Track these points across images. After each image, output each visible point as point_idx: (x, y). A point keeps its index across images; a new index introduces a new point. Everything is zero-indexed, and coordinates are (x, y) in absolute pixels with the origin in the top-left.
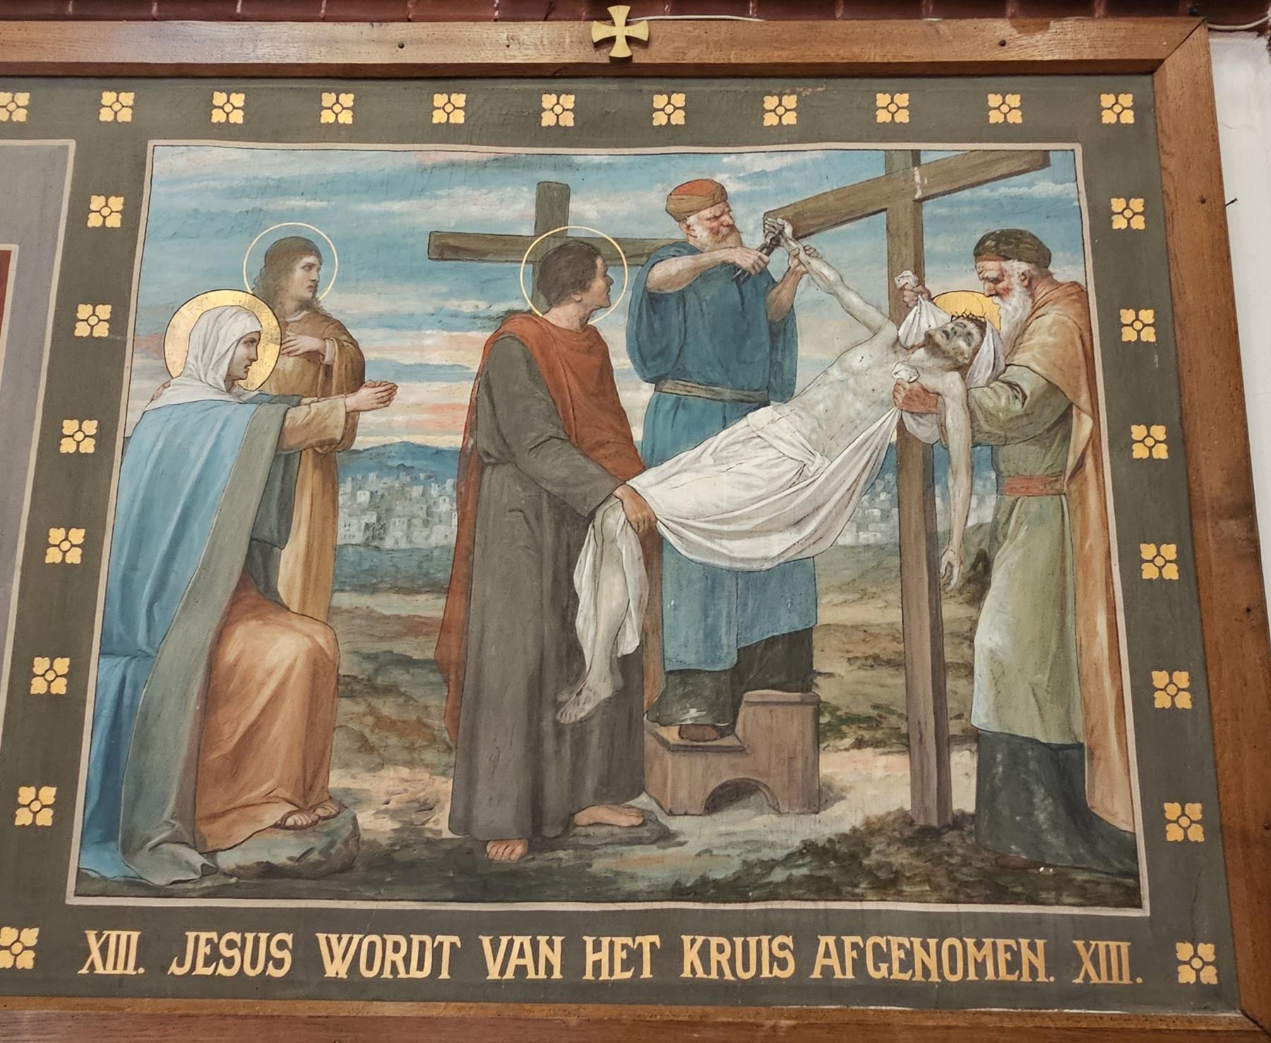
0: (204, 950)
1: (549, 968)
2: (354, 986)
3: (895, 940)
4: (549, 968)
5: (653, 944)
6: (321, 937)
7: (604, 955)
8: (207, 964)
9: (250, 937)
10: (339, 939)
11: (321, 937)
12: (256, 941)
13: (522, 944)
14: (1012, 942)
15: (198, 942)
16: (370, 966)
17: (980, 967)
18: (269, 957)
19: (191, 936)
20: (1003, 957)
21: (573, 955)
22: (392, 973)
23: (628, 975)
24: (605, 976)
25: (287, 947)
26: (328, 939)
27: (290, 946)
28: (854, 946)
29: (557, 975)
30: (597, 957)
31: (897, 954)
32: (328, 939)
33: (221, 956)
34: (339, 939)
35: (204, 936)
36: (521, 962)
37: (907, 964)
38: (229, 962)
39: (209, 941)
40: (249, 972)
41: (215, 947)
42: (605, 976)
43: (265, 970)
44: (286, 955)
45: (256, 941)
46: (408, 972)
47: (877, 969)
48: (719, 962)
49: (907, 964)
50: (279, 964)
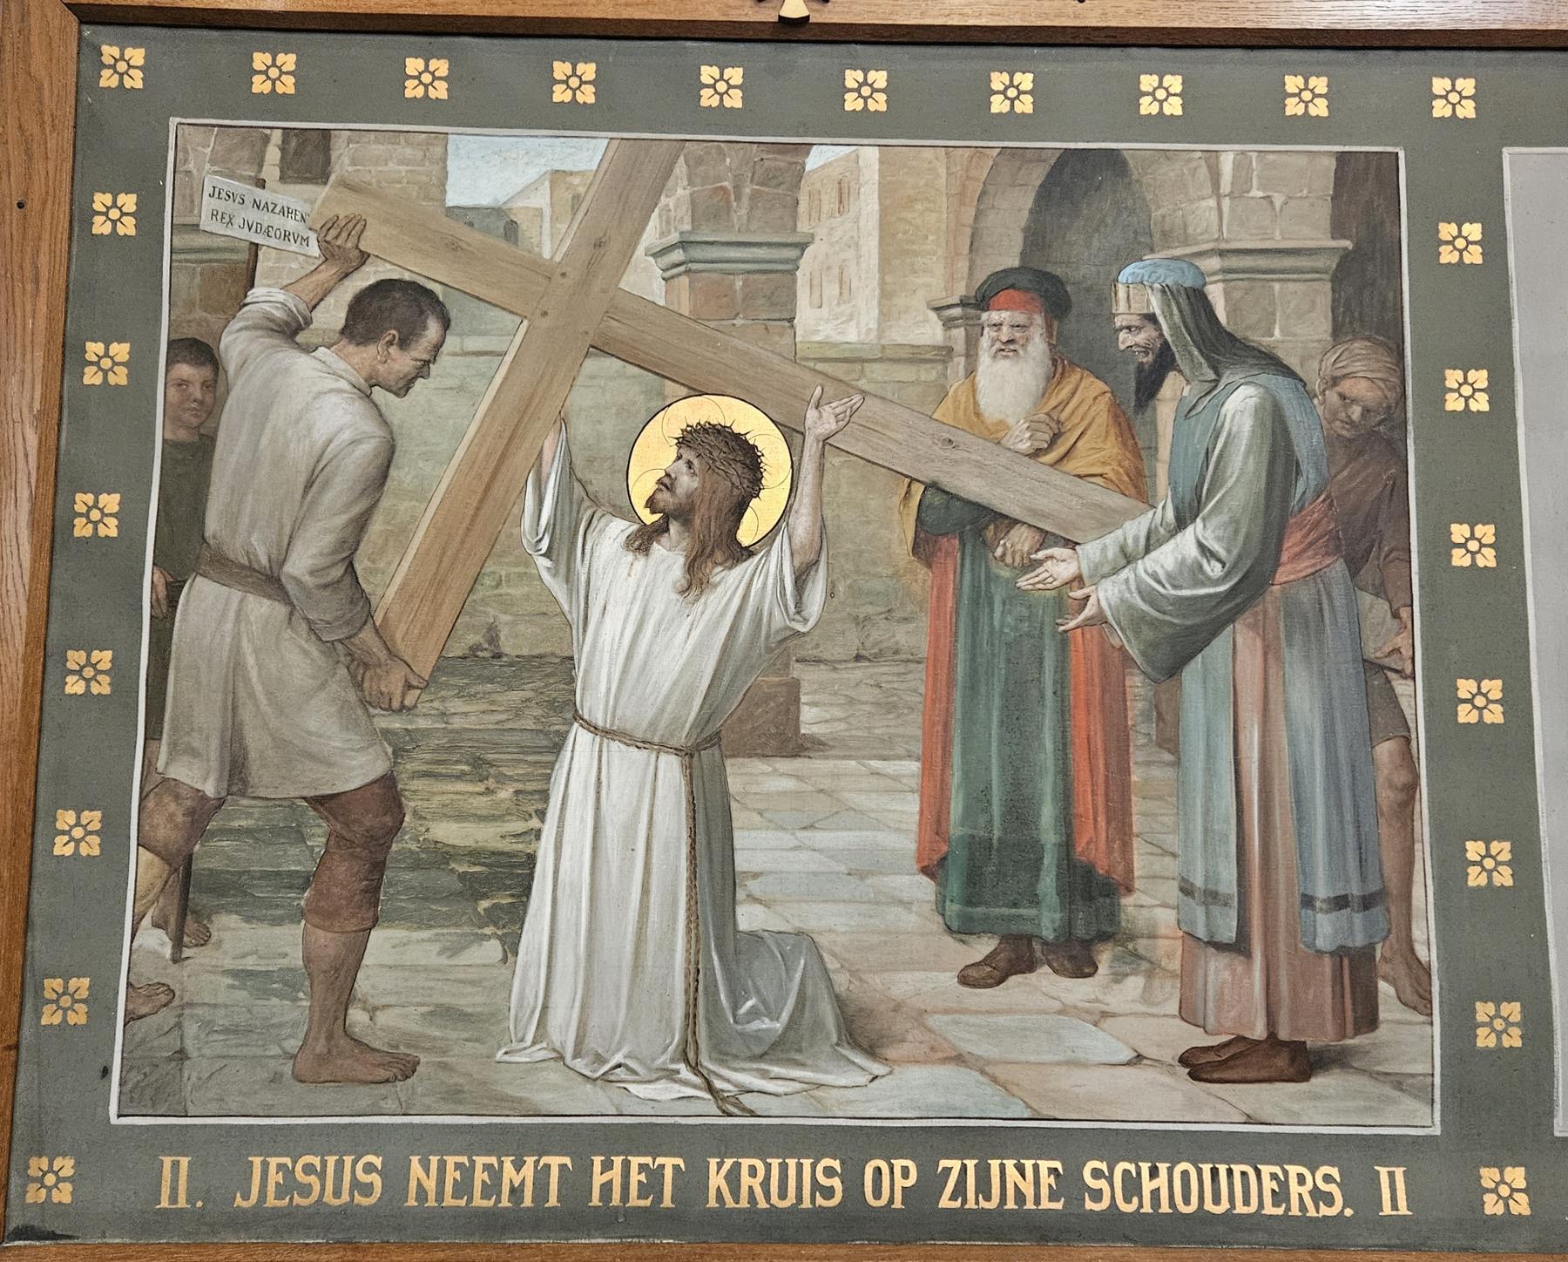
0: (275, 1177)
39: (280, 1167)
41: (288, 1173)
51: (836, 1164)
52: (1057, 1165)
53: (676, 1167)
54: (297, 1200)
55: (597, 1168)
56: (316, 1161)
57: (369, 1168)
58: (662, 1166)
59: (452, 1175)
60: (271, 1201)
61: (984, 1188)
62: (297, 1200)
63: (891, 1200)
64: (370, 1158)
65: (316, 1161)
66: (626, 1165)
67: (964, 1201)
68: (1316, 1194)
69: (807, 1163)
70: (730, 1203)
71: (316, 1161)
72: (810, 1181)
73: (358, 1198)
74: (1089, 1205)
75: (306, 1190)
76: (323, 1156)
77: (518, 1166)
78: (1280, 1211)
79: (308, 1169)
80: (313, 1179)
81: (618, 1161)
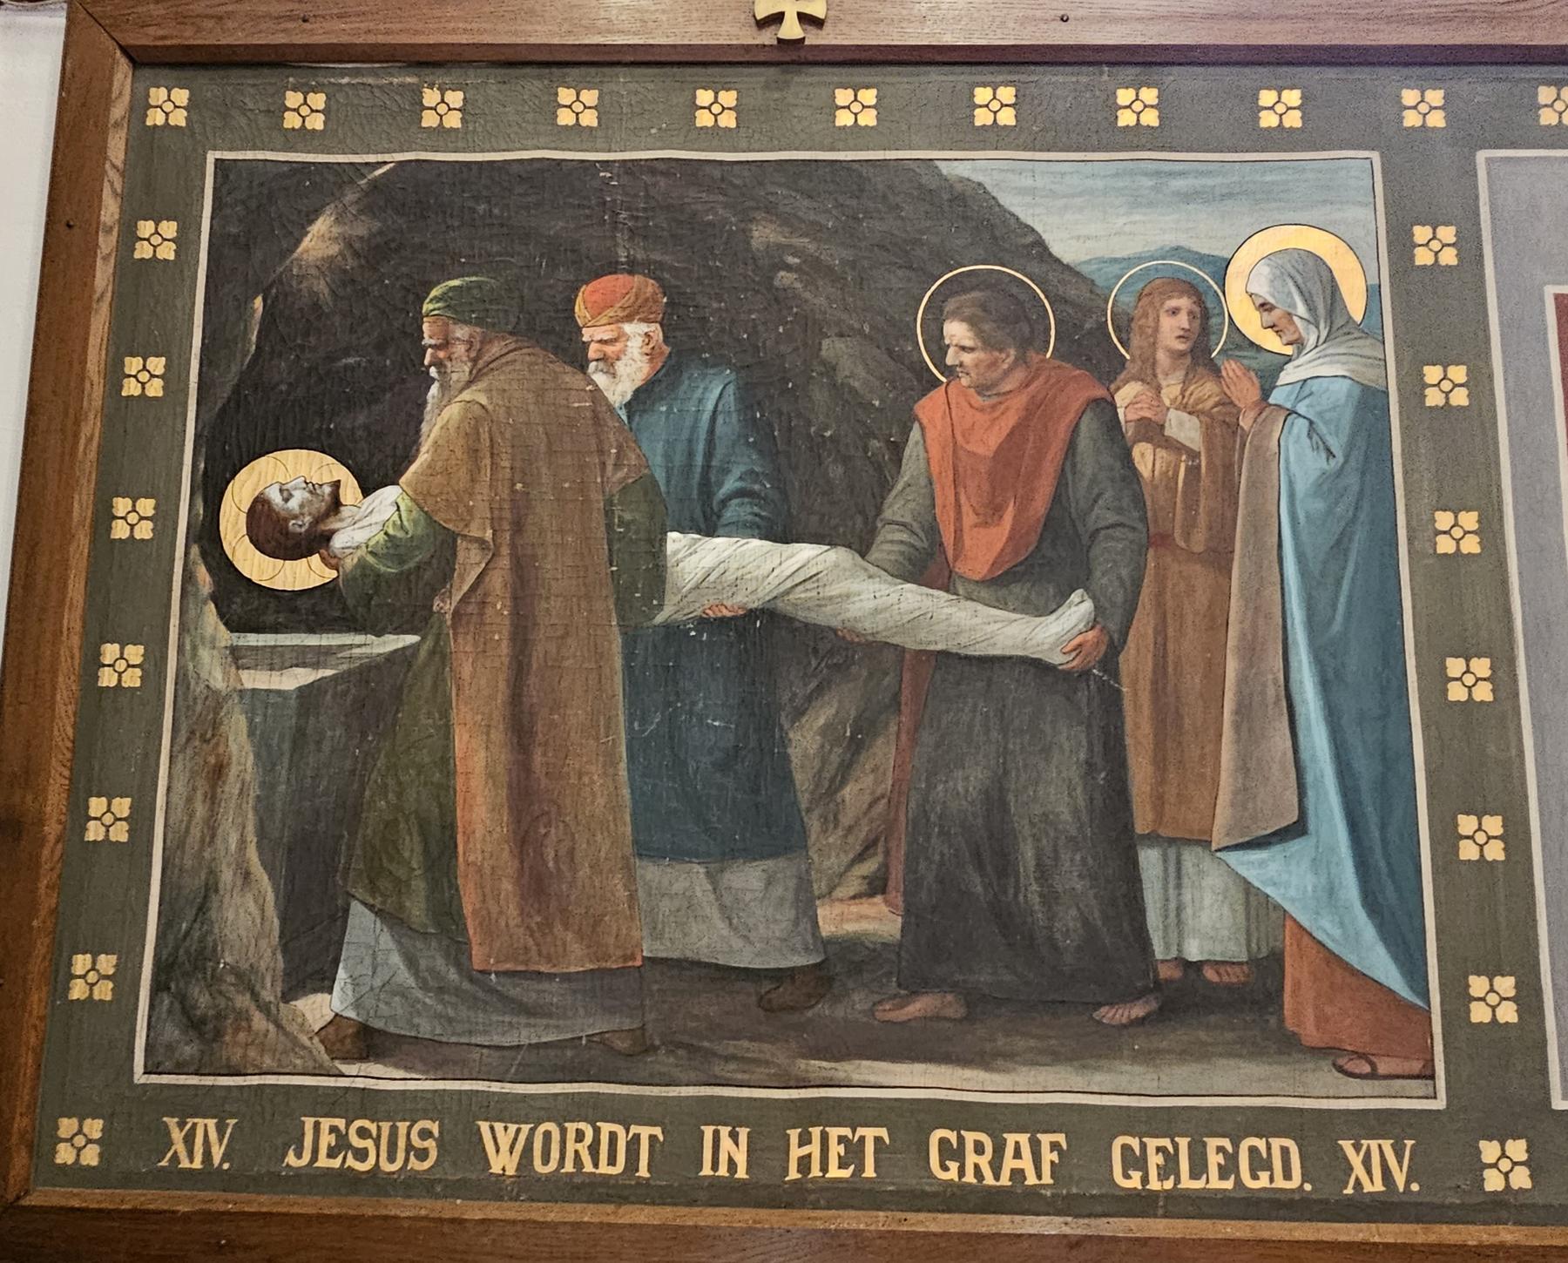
0: (327, 1140)
1: (732, 1165)
2: (526, 1184)
3: (1152, 1143)
4: (732, 1165)
5: (878, 1140)
6: (484, 1126)
8: (332, 1154)
10: (506, 1128)
13: (1017, 1143)
14: (1166, 1142)
15: (319, 1132)
16: (546, 1160)
18: (409, 1147)
19: (309, 1122)
20: (836, 1149)
25: (370, 1136)
26: (492, 1128)
27: (436, 1133)
29: (741, 1173)
31: (1155, 1160)
32: (492, 1128)
33: (350, 1146)
34: (506, 1128)
35: (326, 1123)
36: (1017, 1164)
38: (361, 1155)
43: (407, 1160)
44: (430, 1144)
46: (596, 1165)
48: (576, 1152)
50: (422, 1154)
51: (435, 1128)
52: (1061, 1138)
53: (878, 1140)
54: (351, 1162)
55: (794, 1140)
57: (425, 1134)
58: (862, 1139)
60: (323, 1162)
62: (351, 1162)
64: (427, 1124)
65: (372, 1127)
67: (860, 1168)
68: (958, 1154)
70: (989, 1180)
71: (372, 1127)
75: (361, 1155)
76: (394, 1121)
79: (363, 1133)
80: (369, 1144)
81: (816, 1132)
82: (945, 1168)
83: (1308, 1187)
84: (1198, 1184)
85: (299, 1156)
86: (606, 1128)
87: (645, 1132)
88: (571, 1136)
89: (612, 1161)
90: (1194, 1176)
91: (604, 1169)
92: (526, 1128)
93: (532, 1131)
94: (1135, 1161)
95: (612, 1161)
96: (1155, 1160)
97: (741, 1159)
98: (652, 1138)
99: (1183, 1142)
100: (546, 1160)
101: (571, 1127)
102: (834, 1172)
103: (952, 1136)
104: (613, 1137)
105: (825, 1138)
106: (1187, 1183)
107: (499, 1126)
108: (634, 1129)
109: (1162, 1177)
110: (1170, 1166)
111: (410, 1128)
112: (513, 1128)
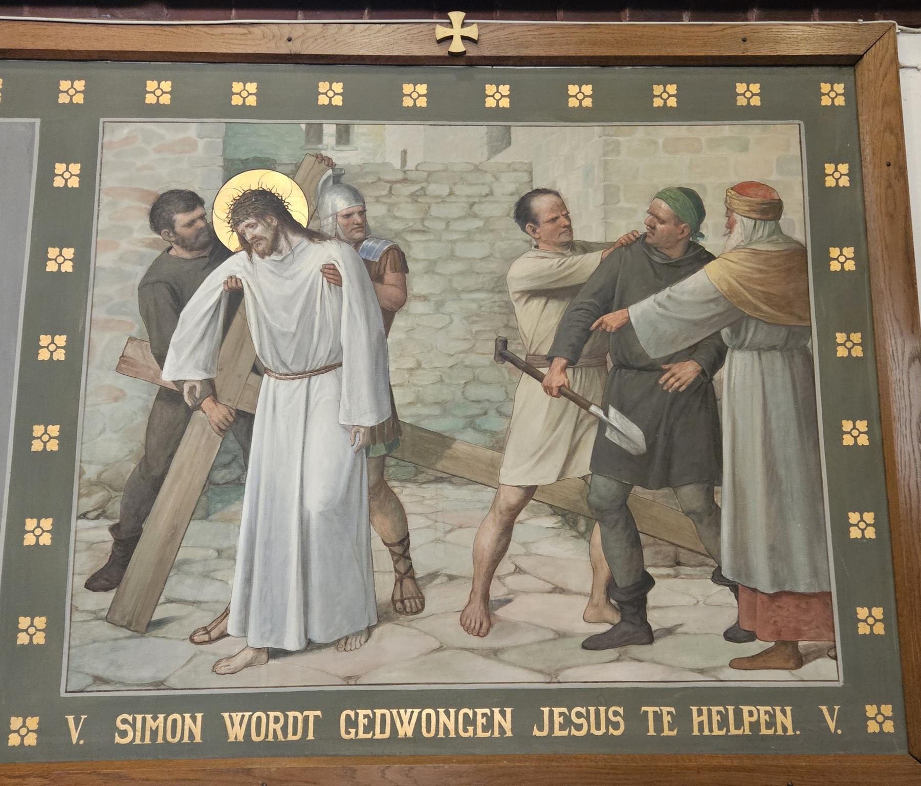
7: (704, 718)
9: (139, 717)
11: (546, 710)
12: (597, 713)
17: (154, 733)
21: (682, 719)
22: (699, 731)
23: (488, 734)
24: (706, 732)
26: (231, 717)
28: (719, 712)
30: (701, 719)
32: (231, 717)
33: (117, 729)
37: (489, 726)
40: (594, 731)
42: (706, 732)
45: (597, 713)
47: (348, 733)
49: (489, 726)
56: (583, 711)
59: (716, 718)
61: (739, 723)
63: (267, 736)
66: (710, 711)
69: (602, 709)
72: (606, 723)
73: (611, 731)
74: (118, 739)
77: (155, 719)
78: (723, 733)
82: (348, 733)
83: (798, 733)
84: (740, 732)
85: (541, 729)
86: (291, 714)
87: (311, 714)
88: (272, 719)
89: (295, 733)
90: (737, 727)
91: (291, 737)
92: (247, 714)
93: (250, 717)
94: (352, 723)
95: (295, 733)
96: (481, 721)
97: (507, 726)
98: (316, 717)
99: (731, 709)
100: (258, 735)
101: (272, 714)
102: (716, 732)
103: (470, 712)
104: (295, 718)
105: (710, 711)
106: (733, 732)
107: (233, 715)
108: (306, 713)
109: (366, 731)
110: (723, 723)
111: (607, 712)
112: (240, 714)
